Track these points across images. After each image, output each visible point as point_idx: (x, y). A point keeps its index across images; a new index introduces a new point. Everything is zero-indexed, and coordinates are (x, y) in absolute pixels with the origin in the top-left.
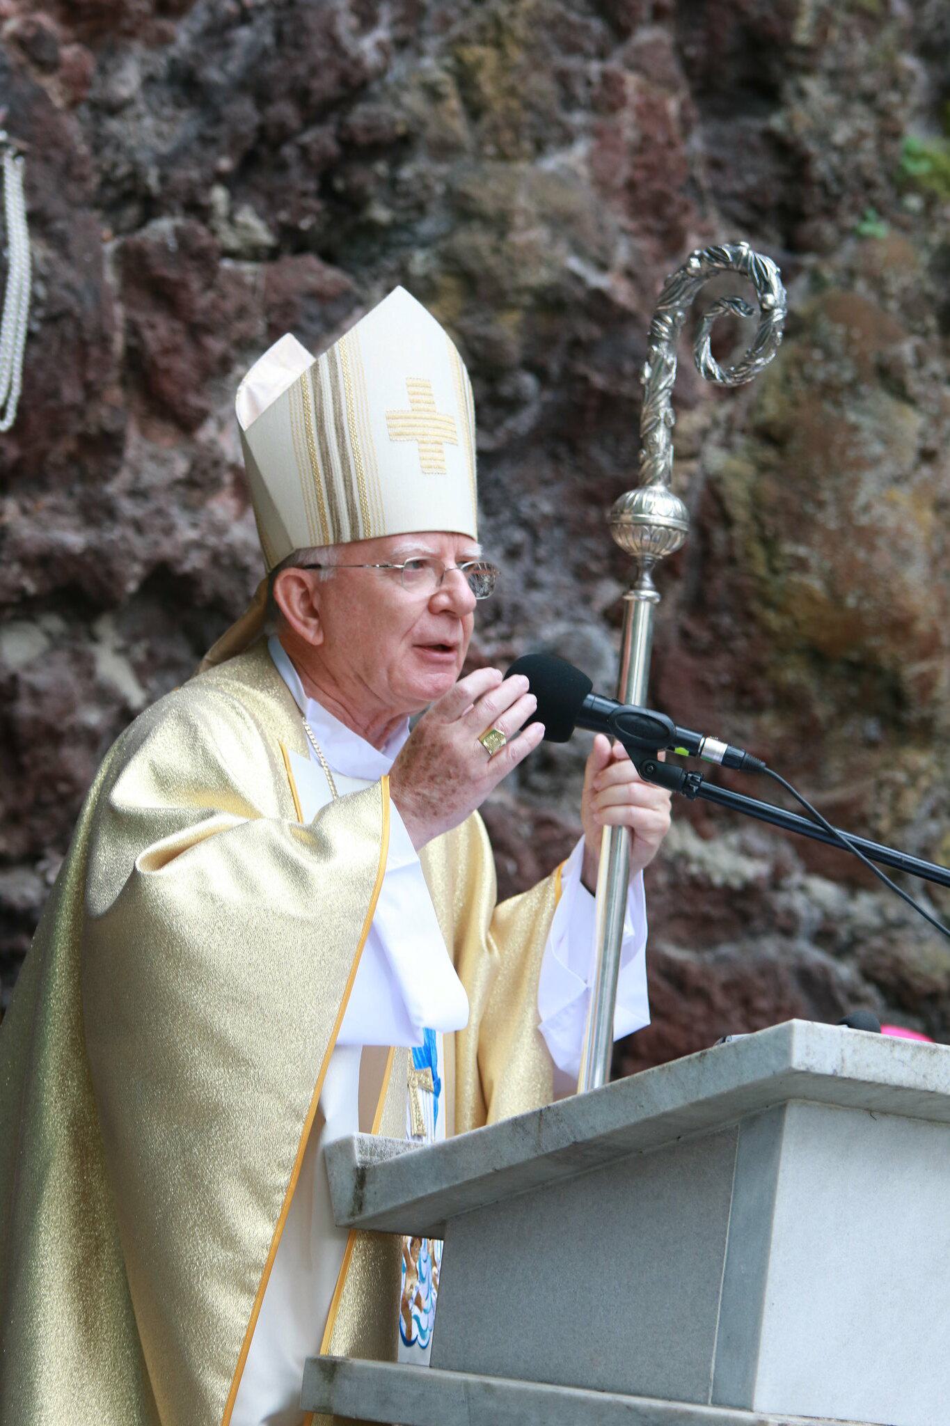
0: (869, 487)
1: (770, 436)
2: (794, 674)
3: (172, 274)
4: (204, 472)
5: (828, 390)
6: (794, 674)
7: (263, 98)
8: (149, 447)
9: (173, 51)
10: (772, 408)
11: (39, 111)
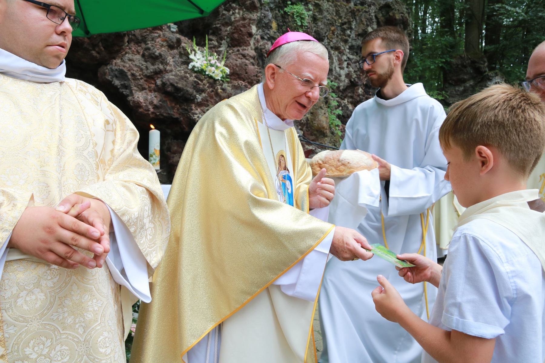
0: (320, 117)
1: (312, 113)
2: (315, 132)
5: (316, 109)
6: (315, 132)
10: (312, 111)
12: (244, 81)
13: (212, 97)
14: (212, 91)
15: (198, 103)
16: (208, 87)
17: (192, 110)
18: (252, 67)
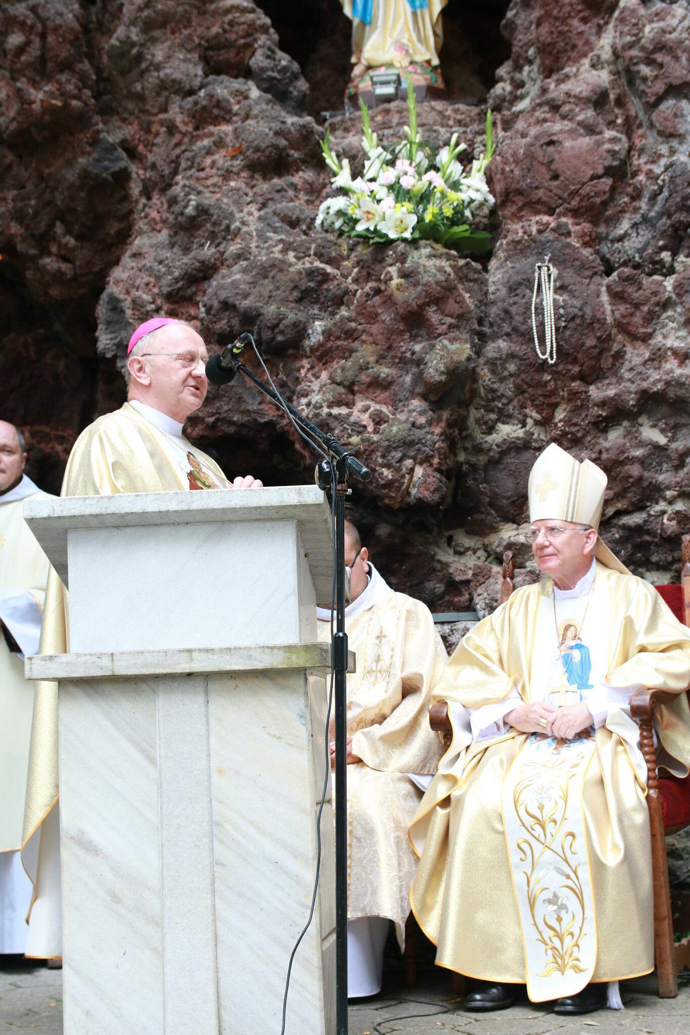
3: (619, 289)
4: (654, 354)
7: (669, 216)
8: (636, 352)
9: (642, 211)
11: (567, 251)
12: (551, 212)
13: (372, 318)
14: (378, 291)
15: (313, 350)
16: (356, 281)
17: (297, 381)
18: (585, 142)
